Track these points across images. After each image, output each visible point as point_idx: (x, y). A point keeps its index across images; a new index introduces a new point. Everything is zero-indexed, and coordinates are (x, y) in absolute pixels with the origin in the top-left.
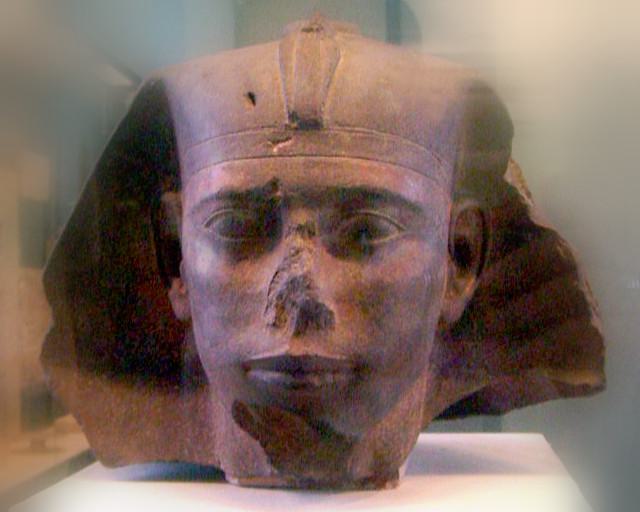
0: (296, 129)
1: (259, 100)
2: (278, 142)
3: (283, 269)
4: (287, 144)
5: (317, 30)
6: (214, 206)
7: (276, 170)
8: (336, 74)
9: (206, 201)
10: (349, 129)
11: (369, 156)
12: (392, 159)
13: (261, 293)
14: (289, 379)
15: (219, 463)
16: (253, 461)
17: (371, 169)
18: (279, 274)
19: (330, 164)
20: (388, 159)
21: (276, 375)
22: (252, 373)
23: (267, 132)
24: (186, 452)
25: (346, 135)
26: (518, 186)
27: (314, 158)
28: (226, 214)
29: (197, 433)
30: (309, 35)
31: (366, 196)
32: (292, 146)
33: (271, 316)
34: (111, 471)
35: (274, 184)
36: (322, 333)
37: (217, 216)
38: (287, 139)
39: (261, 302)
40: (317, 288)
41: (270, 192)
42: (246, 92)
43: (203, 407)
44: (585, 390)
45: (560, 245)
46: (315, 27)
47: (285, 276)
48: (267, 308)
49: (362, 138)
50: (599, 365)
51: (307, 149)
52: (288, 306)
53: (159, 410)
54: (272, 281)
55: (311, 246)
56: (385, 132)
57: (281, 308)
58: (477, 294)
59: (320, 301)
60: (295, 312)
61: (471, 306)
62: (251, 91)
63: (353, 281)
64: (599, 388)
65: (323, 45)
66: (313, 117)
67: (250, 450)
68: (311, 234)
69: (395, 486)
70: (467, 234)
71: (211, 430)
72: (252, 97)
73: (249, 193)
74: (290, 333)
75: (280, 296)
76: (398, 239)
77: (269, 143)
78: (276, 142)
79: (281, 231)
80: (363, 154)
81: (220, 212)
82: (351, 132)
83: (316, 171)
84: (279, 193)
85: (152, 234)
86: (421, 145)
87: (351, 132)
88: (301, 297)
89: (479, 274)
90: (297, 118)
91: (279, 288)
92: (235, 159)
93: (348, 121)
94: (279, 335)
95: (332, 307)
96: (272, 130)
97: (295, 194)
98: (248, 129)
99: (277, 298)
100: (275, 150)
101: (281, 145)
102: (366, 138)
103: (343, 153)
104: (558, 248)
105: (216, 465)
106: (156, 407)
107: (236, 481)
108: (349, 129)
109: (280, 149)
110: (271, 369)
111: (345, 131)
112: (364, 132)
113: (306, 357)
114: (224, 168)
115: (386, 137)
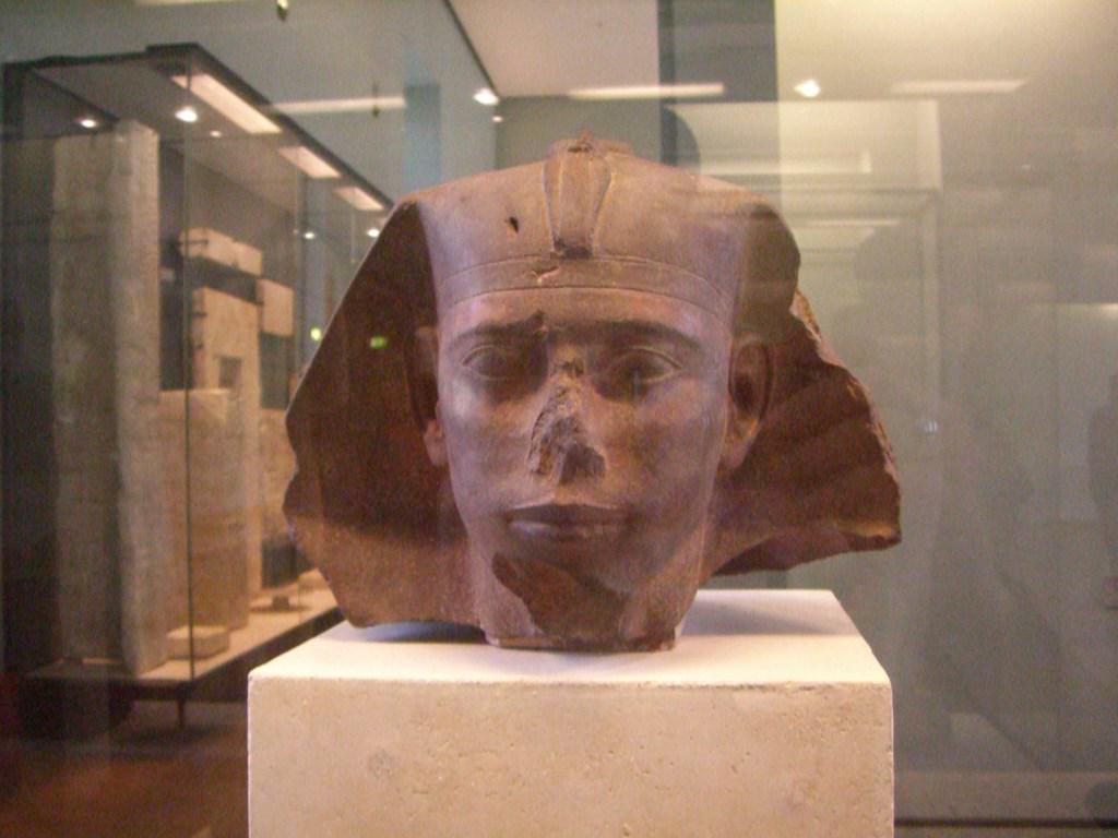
0: (563, 258)
1: (523, 226)
2: (543, 272)
3: (548, 411)
4: (554, 274)
6: (472, 341)
8: (607, 197)
9: (464, 336)
11: (643, 287)
12: (668, 291)
13: (524, 437)
14: (555, 531)
15: (479, 622)
16: (516, 620)
17: (644, 301)
18: (544, 416)
19: (599, 296)
20: (663, 290)
21: (540, 527)
22: (515, 525)
24: (442, 610)
25: (617, 264)
26: (805, 320)
28: (486, 350)
30: (577, 155)
31: (642, 331)
32: (557, 276)
34: (360, 631)
35: (539, 318)
36: (591, 480)
37: (475, 354)
38: (554, 268)
40: (586, 431)
42: (508, 217)
44: (880, 543)
45: (852, 385)
46: (583, 146)
47: (551, 418)
48: (531, 453)
50: (893, 516)
52: (554, 451)
53: (413, 564)
54: (537, 424)
55: (579, 386)
56: (659, 260)
57: (546, 453)
58: (760, 437)
59: (589, 445)
60: (562, 458)
61: (754, 450)
64: (894, 541)
65: (591, 165)
66: (581, 244)
67: (512, 608)
68: (579, 372)
69: (670, 647)
70: (750, 372)
71: (469, 586)
72: (514, 223)
73: (511, 327)
75: (545, 440)
76: (673, 378)
77: (534, 273)
78: (540, 272)
79: (546, 370)
82: (622, 260)
83: (585, 304)
84: (544, 328)
85: (405, 373)
86: (700, 276)
87: (622, 260)
88: (568, 441)
89: (762, 416)
90: (564, 246)
91: (544, 430)
92: (495, 290)
94: (544, 482)
95: (602, 451)
96: (536, 259)
97: (562, 329)
98: (510, 258)
99: (542, 443)
100: (540, 281)
101: (546, 275)
102: (639, 267)
103: (614, 284)
104: (849, 387)
105: (476, 625)
107: (497, 642)
109: (545, 279)
111: (616, 260)
112: (638, 262)
113: (574, 507)
114: (483, 301)
115: (660, 266)
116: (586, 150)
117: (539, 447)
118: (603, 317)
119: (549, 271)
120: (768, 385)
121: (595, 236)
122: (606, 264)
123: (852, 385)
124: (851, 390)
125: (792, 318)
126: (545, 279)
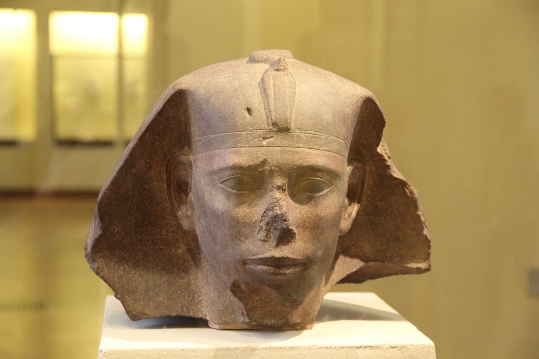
0: (276, 131)
1: (255, 112)
2: (266, 138)
3: (269, 210)
4: (271, 139)
5: (283, 70)
6: (229, 172)
7: (265, 155)
9: (222, 170)
10: (305, 132)
12: (327, 149)
13: (255, 222)
14: (272, 269)
15: (206, 316)
16: (231, 315)
17: (317, 155)
19: (295, 152)
20: (325, 148)
21: (264, 268)
22: (248, 266)
23: (259, 132)
24: (185, 310)
25: (303, 135)
27: (287, 149)
29: (191, 298)
30: (278, 73)
31: (314, 170)
32: (273, 141)
33: (262, 236)
34: (135, 322)
35: (264, 162)
37: (229, 179)
38: (272, 137)
39: (255, 227)
40: (289, 220)
41: (262, 167)
43: (193, 282)
44: (419, 271)
45: (408, 189)
47: (271, 214)
49: (311, 137)
50: (427, 257)
51: (282, 143)
52: (272, 230)
53: (166, 284)
55: (284, 197)
57: (268, 231)
59: (291, 227)
60: (277, 233)
62: (249, 107)
63: (305, 216)
64: (427, 270)
66: (285, 125)
67: (230, 308)
68: (284, 190)
73: (250, 166)
74: (274, 244)
75: (268, 224)
77: (261, 139)
78: (265, 138)
80: (311, 147)
81: (233, 177)
82: (305, 133)
83: (288, 156)
84: (267, 167)
85: (165, 178)
87: (305, 133)
88: (281, 225)
90: (277, 126)
92: (241, 147)
93: (304, 127)
94: (267, 245)
95: (295, 230)
96: (262, 132)
97: (276, 169)
99: (266, 226)
100: (264, 143)
101: (267, 140)
102: (313, 137)
103: (302, 145)
104: (406, 190)
105: (204, 317)
106: (164, 282)
107: (217, 326)
108: (305, 132)
109: (267, 142)
110: (262, 264)
111: (303, 133)
112: (312, 134)
113: (283, 259)
116: (283, 70)
117: (264, 228)
118: (297, 163)
119: (269, 138)
120: (363, 186)
121: (292, 120)
122: (298, 135)
123: (408, 189)
124: (408, 191)
125: (378, 153)
126: (267, 142)
